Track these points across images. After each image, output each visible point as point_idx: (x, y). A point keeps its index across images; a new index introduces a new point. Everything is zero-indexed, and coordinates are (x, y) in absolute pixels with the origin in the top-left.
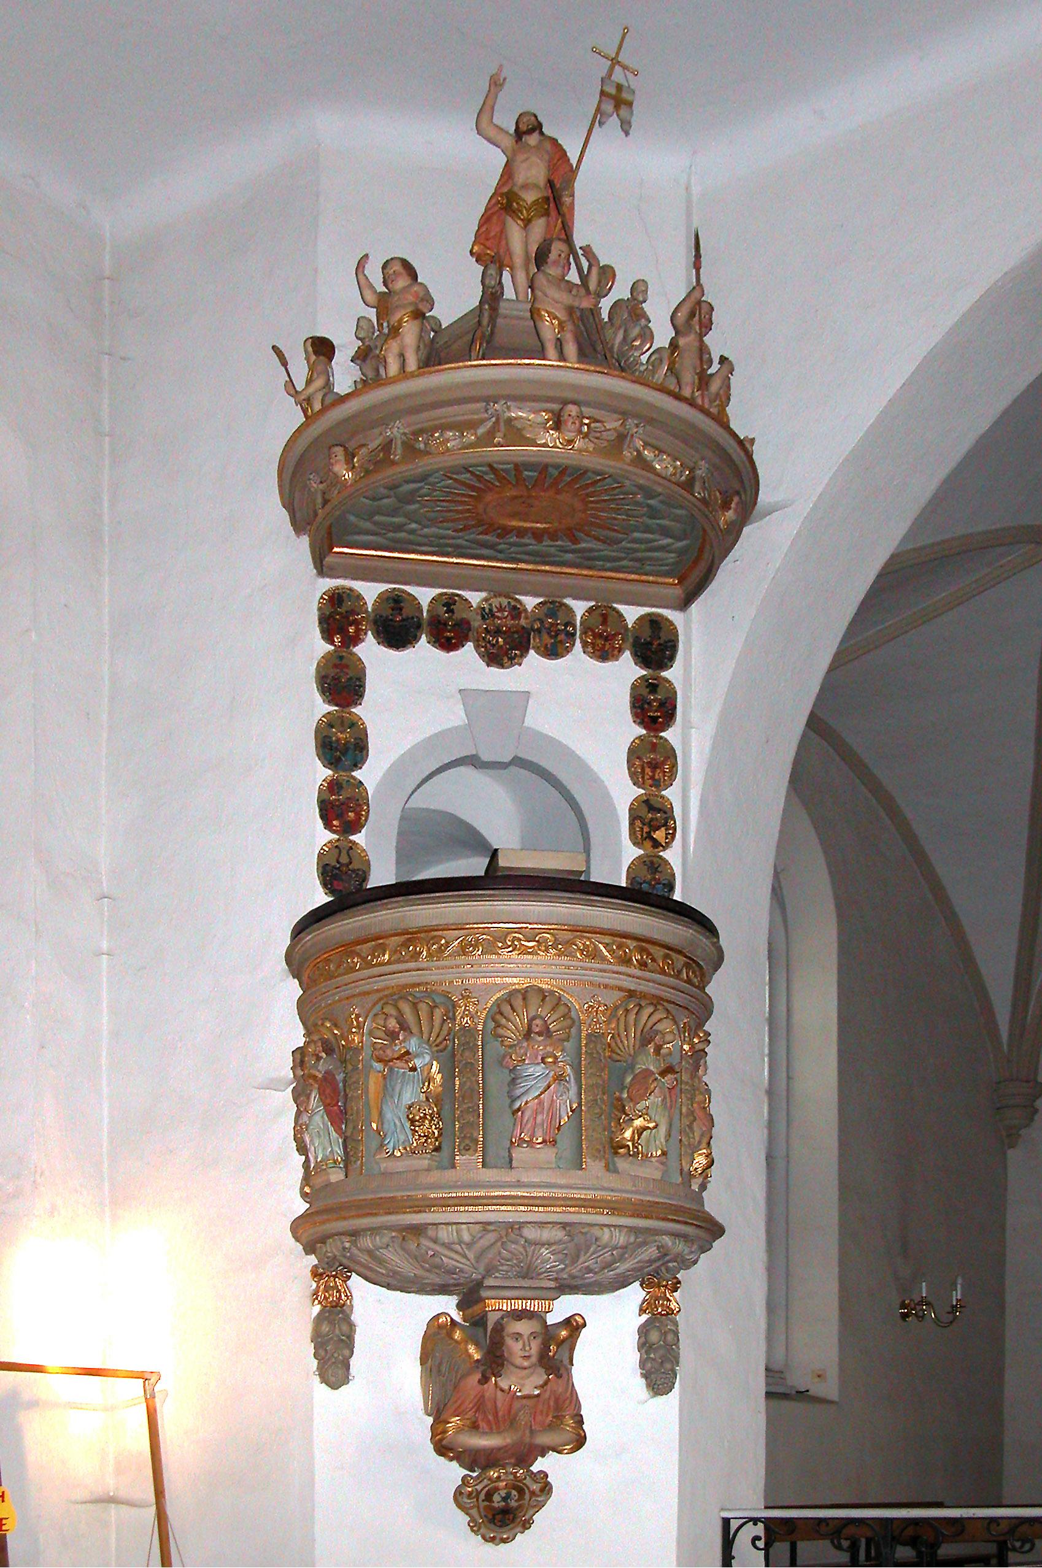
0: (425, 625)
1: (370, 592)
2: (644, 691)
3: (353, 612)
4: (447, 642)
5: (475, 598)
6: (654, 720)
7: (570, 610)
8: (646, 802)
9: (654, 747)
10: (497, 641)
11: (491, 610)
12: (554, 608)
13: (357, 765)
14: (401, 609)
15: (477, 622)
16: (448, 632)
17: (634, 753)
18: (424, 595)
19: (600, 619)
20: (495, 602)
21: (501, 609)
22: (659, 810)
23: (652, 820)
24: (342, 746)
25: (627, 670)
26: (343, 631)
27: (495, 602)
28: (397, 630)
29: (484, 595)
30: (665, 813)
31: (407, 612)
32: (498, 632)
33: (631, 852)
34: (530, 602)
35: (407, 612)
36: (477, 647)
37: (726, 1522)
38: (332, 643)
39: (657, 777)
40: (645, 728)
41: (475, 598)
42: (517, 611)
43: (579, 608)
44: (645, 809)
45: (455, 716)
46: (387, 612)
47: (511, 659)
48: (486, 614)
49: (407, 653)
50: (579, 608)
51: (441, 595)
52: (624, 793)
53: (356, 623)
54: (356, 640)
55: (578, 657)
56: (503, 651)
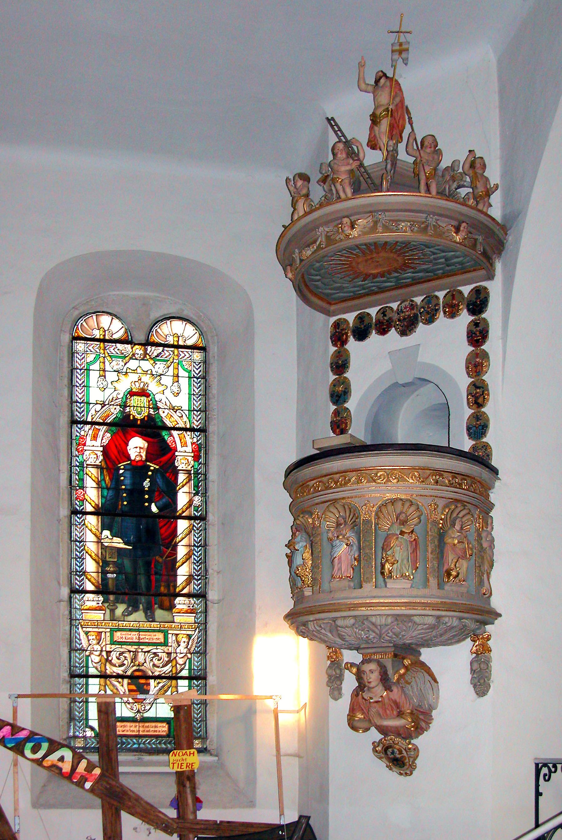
0: (373, 326)
1: (351, 317)
3: (343, 329)
4: (383, 331)
6: (477, 341)
7: (437, 297)
12: (431, 299)
13: (345, 401)
14: (363, 321)
15: (395, 317)
18: (373, 311)
21: (405, 308)
23: (476, 393)
25: (465, 318)
27: (403, 305)
29: (399, 303)
34: (418, 300)
35: (366, 322)
36: (396, 329)
37: (537, 765)
38: (337, 346)
41: (394, 306)
42: (413, 306)
43: (441, 294)
45: (386, 366)
47: (410, 331)
48: (399, 312)
49: (367, 341)
50: (441, 294)
52: (464, 381)
55: (442, 319)
56: (407, 327)
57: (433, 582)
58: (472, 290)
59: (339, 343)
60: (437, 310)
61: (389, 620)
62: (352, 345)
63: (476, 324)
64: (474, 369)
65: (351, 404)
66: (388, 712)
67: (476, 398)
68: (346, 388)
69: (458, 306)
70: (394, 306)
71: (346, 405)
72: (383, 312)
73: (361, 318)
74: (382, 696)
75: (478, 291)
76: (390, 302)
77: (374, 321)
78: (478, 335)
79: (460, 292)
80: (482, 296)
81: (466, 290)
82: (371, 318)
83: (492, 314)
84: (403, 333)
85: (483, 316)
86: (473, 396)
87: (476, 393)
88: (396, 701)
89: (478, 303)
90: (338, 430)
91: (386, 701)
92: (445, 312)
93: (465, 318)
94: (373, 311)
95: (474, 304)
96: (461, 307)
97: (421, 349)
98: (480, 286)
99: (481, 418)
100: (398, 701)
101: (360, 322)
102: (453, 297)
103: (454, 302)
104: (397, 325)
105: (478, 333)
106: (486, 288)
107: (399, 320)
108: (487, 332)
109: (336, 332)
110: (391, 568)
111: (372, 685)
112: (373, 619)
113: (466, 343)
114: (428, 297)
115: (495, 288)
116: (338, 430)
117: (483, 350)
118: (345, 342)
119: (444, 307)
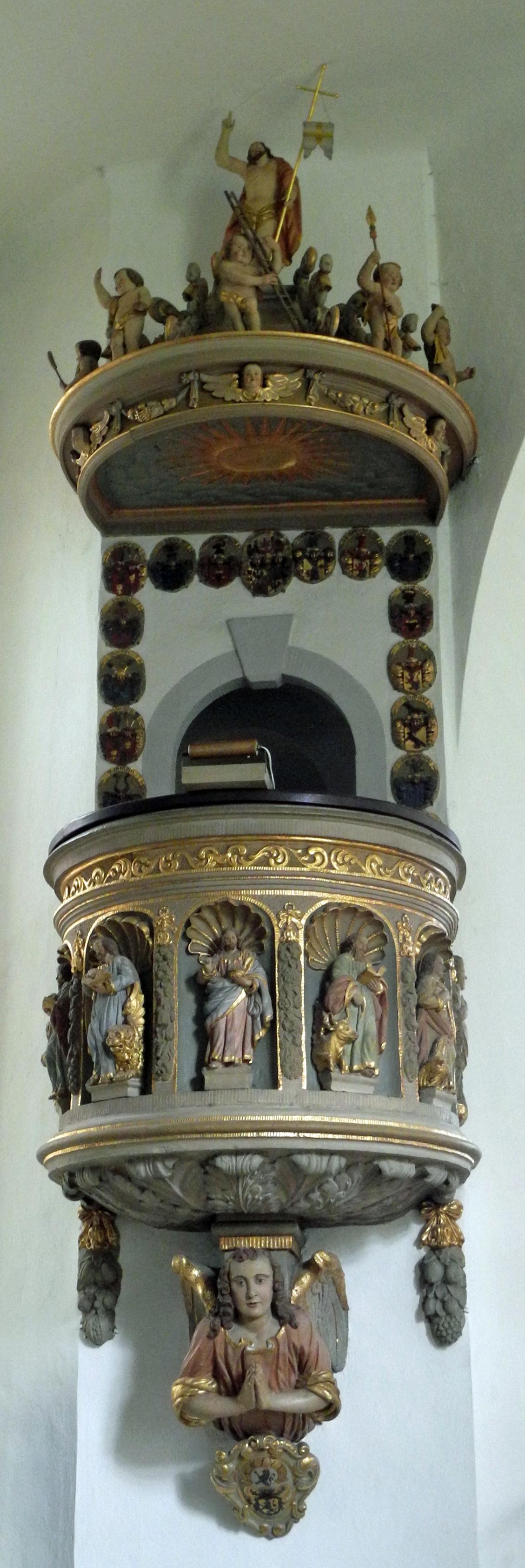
0: (195, 566)
1: (148, 545)
2: (402, 602)
3: (132, 563)
5: (241, 537)
6: (411, 627)
7: (327, 538)
8: (407, 705)
9: (411, 652)
10: (262, 573)
11: (256, 546)
16: (217, 571)
17: (392, 661)
18: (196, 541)
19: (357, 542)
20: (260, 538)
21: (265, 544)
22: (418, 711)
23: (412, 720)
24: (120, 684)
25: (384, 585)
26: (124, 580)
27: (260, 538)
28: (171, 573)
30: (425, 712)
31: (181, 556)
32: (263, 565)
33: (394, 755)
34: (291, 535)
35: (181, 556)
39: (415, 680)
40: (402, 635)
42: (279, 545)
43: (337, 534)
44: (405, 711)
46: (163, 559)
47: (275, 587)
48: (252, 550)
51: (214, 538)
52: (385, 699)
53: (137, 572)
54: (135, 587)
55: (336, 580)
57: (410, 1088)
58: (400, 534)
59: (120, 588)
60: (328, 560)
61: (337, 1163)
62: (149, 596)
63: (408, 597)
64: (407, 674)
65: (145, 707)
66: (281, 1376)
67: (413, 728)
68: (134, 674)
69: (371, 557)
70: (241, 537)
71: (135, 707)
72: (218, 545)
73: (170, 548)
74: (275, 1338)
75: (409, 540)
76: (232, 529)
77: (197, 557)
78: (411, 615)
79: (377, 536)
80: (419, 549)
81: (387, 534)
82: (192, 553)
83: (439, 584)
84: (259, 590)
85: (422, 584)
86: (405, 725)
87: (412, 720)
88: (302, 1348)
89: (411, 561)
90: (115, 753)
91: (284, 1349)
92: (344, 567)
93: (384, 585)
94: (196, 541)
95: (404, 559)
96: (377, 562)
97: (295, 622)
98: (411, 531)
99: (422, 768)
100: (306, 1349)
101: (169, 556)
102: (361, 541)
103: (364, 550)
104: (249, 572)
105: (412, 613)
106: (425, 537)
107: (253, 565)
108: (431, 613)
109: (117, 565)
110: (341, 1049)
111: (257, 1311)
112: (303, 1160)
113: (388, 627)
114: (312, 533)
115: (442, 538)
116: (115, 753)
117: (424, 644)
118: (132, 588)
119: (342, 554)
